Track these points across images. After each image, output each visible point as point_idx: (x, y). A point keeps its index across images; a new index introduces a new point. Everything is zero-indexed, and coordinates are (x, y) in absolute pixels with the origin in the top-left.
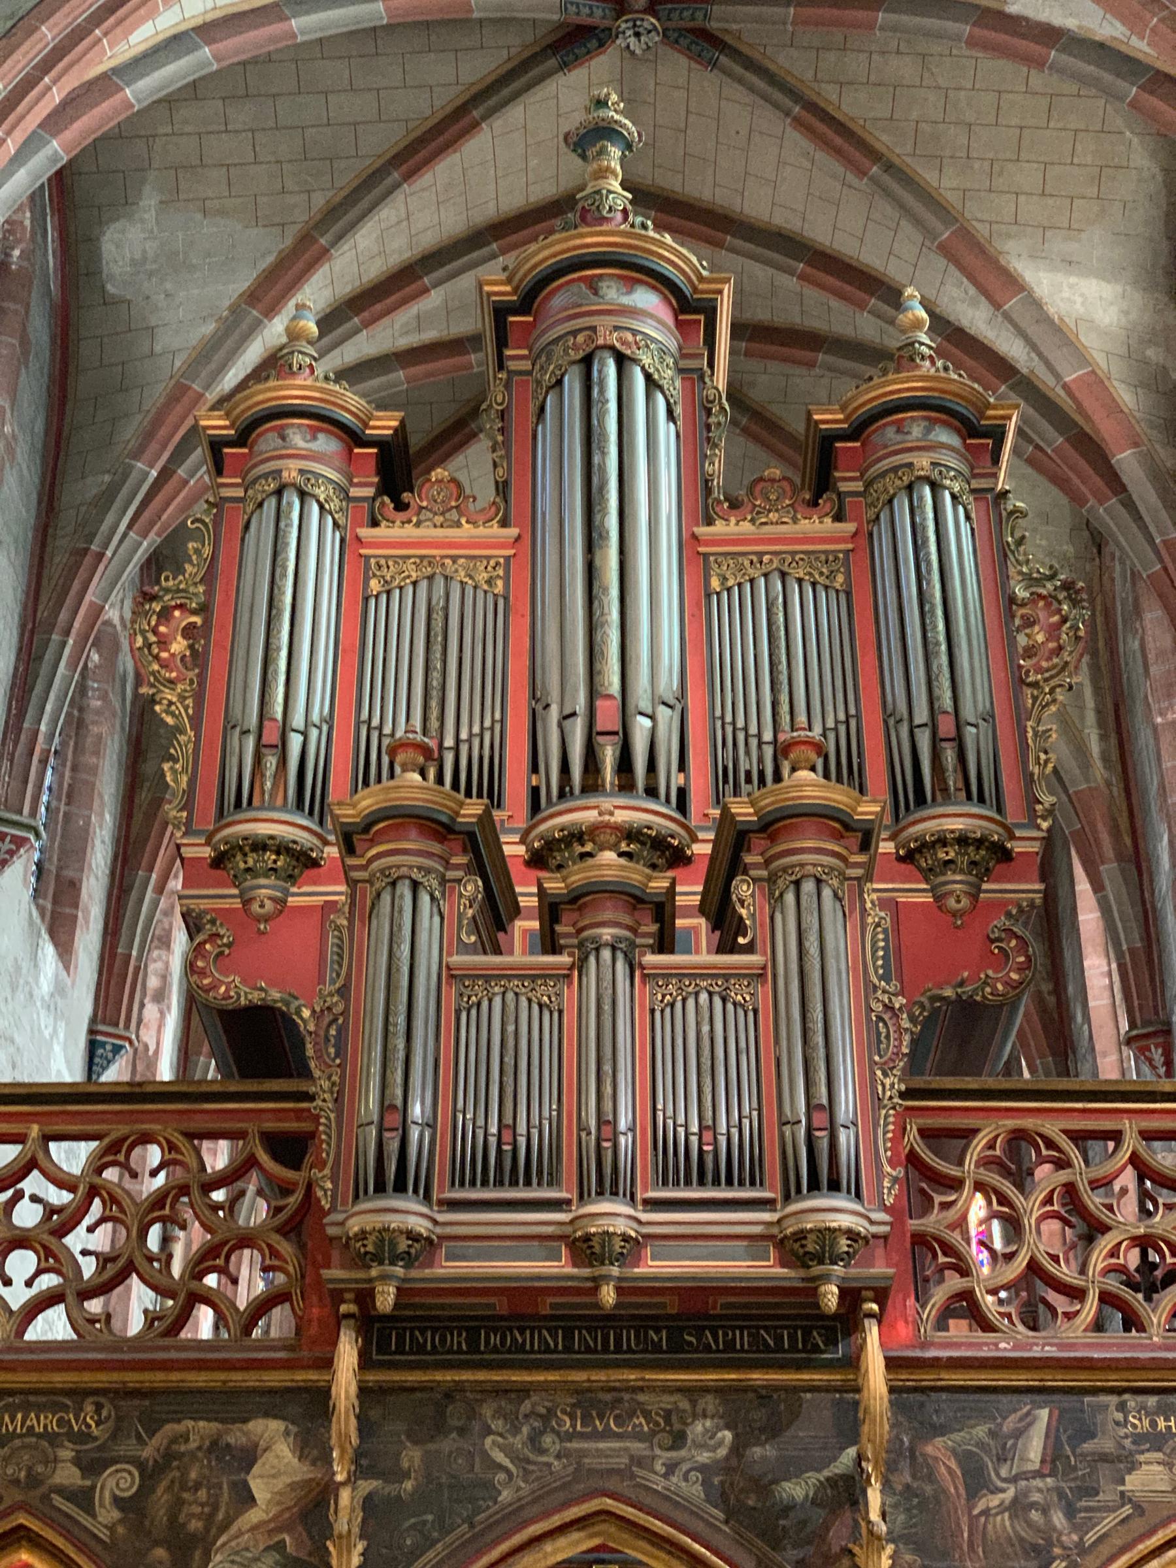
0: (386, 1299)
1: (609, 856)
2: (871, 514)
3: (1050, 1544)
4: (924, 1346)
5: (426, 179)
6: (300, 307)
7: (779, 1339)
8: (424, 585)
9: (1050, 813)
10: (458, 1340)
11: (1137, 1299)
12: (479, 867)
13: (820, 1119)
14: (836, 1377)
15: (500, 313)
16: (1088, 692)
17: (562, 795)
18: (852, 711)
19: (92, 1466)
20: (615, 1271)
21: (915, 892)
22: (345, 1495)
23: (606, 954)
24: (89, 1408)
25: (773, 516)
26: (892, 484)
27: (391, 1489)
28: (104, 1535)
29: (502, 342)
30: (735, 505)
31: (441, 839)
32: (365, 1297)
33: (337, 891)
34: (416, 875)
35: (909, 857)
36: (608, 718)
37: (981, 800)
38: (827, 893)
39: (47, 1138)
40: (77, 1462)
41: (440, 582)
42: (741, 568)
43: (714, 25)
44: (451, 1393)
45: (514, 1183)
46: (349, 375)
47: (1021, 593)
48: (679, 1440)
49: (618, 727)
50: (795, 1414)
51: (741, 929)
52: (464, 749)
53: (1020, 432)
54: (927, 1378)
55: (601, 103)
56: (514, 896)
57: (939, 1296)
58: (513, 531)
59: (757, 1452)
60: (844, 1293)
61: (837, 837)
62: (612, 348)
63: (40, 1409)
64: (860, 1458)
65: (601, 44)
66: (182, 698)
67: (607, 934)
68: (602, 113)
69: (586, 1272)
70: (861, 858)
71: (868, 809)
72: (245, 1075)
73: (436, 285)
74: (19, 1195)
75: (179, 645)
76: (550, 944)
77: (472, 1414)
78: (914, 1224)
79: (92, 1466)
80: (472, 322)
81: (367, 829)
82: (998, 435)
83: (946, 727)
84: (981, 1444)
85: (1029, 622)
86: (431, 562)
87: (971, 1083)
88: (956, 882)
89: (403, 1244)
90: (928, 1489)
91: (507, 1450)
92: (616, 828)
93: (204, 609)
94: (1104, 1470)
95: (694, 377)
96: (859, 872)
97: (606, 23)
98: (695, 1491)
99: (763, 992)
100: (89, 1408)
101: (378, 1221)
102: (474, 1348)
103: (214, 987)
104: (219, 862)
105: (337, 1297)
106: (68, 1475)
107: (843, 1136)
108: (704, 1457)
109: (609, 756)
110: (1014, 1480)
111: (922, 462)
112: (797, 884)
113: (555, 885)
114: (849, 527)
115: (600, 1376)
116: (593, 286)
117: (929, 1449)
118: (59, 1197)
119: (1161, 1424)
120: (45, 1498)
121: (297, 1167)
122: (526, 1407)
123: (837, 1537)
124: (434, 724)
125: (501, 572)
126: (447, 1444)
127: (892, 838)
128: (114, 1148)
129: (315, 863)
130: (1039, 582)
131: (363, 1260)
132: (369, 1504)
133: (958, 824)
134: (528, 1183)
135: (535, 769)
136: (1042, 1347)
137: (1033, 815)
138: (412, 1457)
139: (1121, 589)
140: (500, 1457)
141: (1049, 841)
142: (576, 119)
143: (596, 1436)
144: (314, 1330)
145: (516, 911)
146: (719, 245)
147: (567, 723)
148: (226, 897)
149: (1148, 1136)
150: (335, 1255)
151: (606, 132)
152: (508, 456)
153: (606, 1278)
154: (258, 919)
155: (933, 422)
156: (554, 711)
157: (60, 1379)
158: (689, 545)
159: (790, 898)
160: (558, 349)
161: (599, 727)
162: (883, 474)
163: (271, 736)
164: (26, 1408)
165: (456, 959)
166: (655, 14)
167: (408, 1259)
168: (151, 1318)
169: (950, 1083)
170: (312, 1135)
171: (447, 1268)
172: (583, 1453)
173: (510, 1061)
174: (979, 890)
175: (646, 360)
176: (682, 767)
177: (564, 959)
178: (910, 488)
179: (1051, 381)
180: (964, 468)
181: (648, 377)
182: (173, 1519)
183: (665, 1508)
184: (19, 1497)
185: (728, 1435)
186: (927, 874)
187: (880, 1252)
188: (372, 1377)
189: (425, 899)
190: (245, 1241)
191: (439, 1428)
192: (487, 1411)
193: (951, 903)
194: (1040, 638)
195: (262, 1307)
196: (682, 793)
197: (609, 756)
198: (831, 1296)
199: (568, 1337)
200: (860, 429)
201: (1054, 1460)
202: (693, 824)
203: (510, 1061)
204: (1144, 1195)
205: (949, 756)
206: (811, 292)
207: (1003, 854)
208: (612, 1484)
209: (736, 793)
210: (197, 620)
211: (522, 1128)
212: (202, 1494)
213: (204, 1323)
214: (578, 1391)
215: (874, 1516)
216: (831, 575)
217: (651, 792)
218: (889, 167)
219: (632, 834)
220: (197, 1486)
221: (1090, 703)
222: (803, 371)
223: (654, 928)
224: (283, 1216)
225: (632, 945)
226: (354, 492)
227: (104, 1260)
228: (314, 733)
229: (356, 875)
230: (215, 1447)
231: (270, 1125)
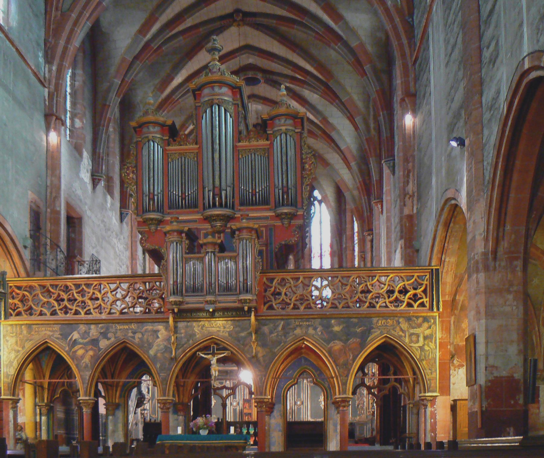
0: (176, 310)
18: (268, 184)
32: (173, 310)
42: (245, 152)
57: (267, 305)
74: (117, 293)
78: (264, 294)
88: (286, 222)
89: (178, 303)
104: (144, 222)
105: (169, 310)
114: (268, 142)
118: (124, 293)
119: (301, 323)
125: (196, 156)
136: (284, 312)
147: (209, 192)
148: (146, 229)
156: (207, 189)
158: (234, 147)
174: (290, 222)
181: (225, 110)
198: (246, 308)
216: (265, 153)
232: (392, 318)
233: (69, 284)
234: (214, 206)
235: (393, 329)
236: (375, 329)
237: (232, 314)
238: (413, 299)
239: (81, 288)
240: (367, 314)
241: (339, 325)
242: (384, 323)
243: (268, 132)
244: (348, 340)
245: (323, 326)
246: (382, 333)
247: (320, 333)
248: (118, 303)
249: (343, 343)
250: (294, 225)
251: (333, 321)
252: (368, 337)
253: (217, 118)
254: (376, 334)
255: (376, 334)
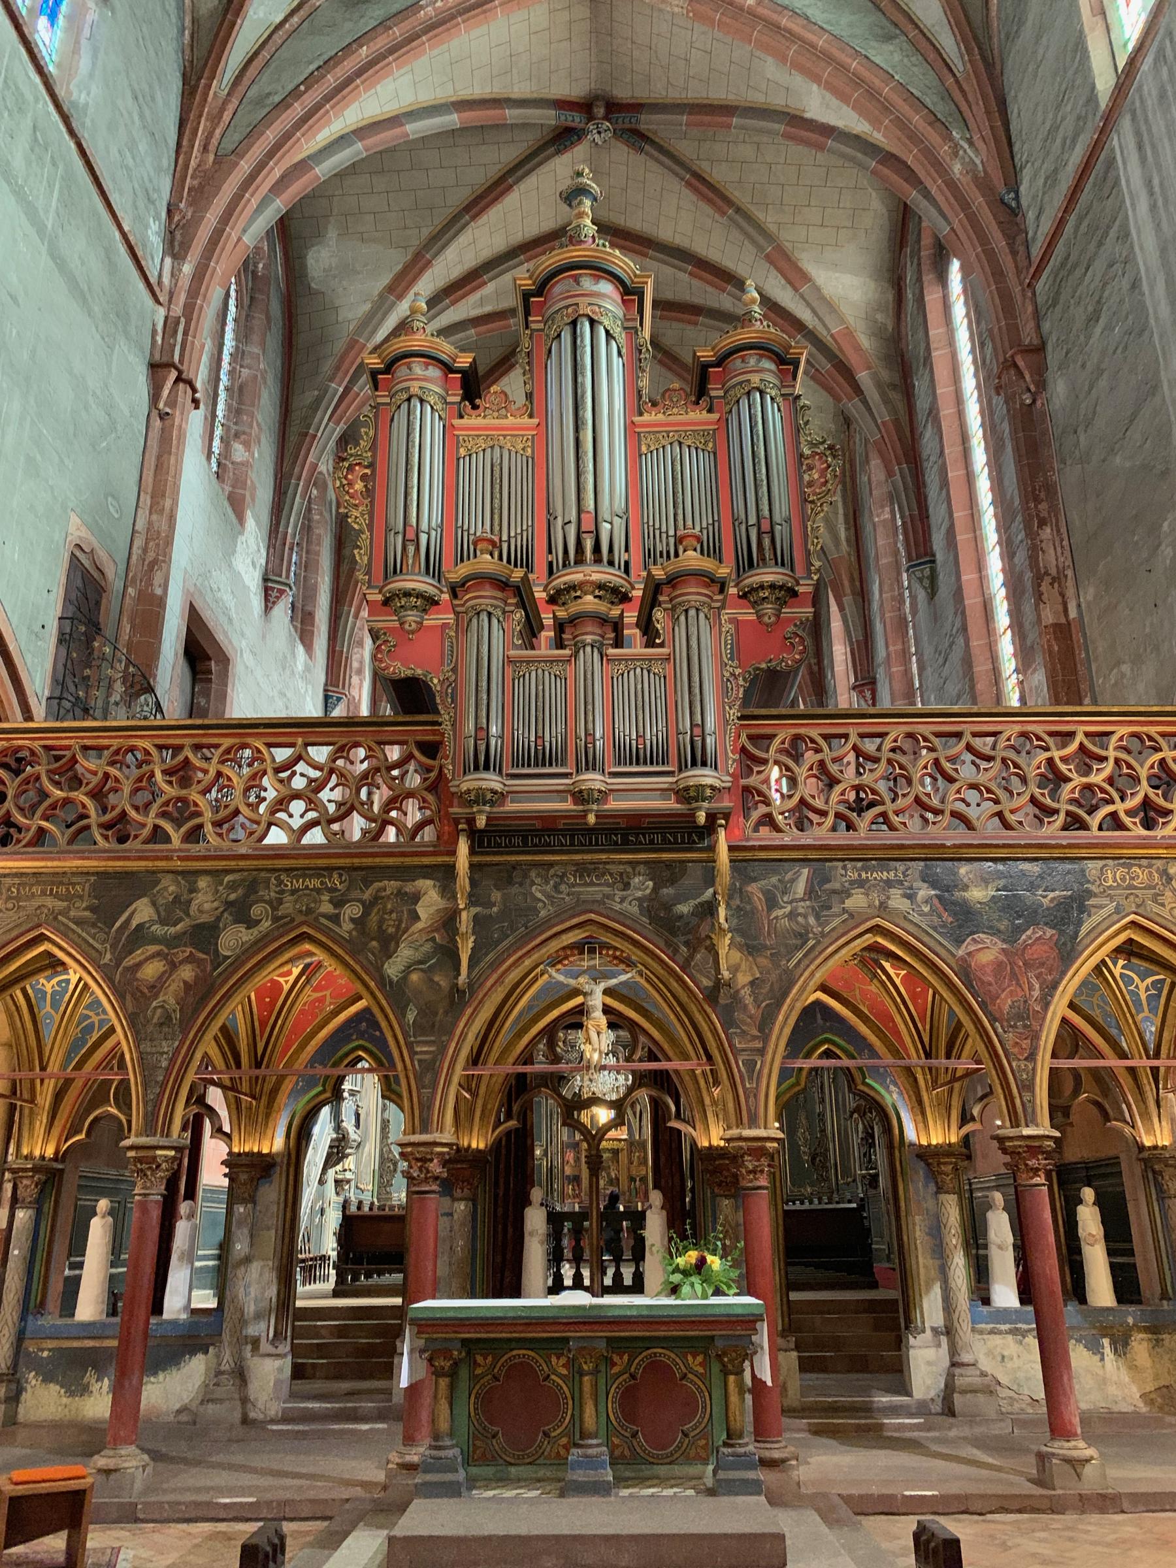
0: (481, 822)
1: (589, 598)
2: (728, 408)
3: (807, 932)
4: (748, 840)
5: (484, 219)
6: (416, 294)
7: (676, 838)
8: (489, 451)
9: (818, 570)
10: (517, 841)
11: (853, 816)
12: (522, 604)
13: (697, 731)
14: (704, 855)
15: (526, 296)
16: (840, 505)
17: (564, 566)
19: (338, 903)
20: (595, 807)
21: (747, 614)
22: (464, 915)
23: (588, 649)
24: (335, 876)
25: (675, 410)
26: (739, 392)
27: (487, 911)
28: (346, 936)
29: (527, 313)
30: (654, 404)
31: (502, 590)
32: (471, 821)
33: (449, 618)
34: (490, 609)
35: (744, 596)
36: (588, 524)
37: (783, 565)
38: (702, 615)
39: (307, 745)
40: (331, 901)
41: (497, 450)
42: (658, 440)
43: (642, 127)
44: (515, 866)
45: (544, 765)
46: (444, 332)
47: (807, 452)
48: (627, 886)
49: (593, 528)
50: (684, 872)
51: (658, 635)
52: (513, 541)
53: (808, 361)
54: (748, 855)
55: (579, 174)
56: (541, 620)
57: (755, 815)
58: (535, 421)
59: (665, 891)
60: (708, 816)
61: (707, 586)
62: (588, 316)
63: (310, 877)
64: (715, 893)
65: (579, 139)
66: (362, 515)
67: (589, 639)
68: (580, 180)
69: (581, 808)
70: (720, 597)
71: (724, 571)
72: (407, 711)
73: (491, 280)
74: (294, 773)
75: (359, 486)
76: (560, 644)
77: (525, 876)
79: (338, 903)
80: (511, 301)
81: (463, 585)
82: (796, 363)
83: (765, 526)
84: (775, 886)
85: (810, 468)
86: (492, 438)
87: (774, 711)
88: (769, 609)
89: (489, 796)
90: (748, 907)
91: (543, 892)
92: (592, 583)
93: (371, 465)
94: (835, 898)
95: (632, 331)
96: (718, 605)
97: (582, 125)
98: (634, 909)
99: (669, 667)
100: (335, 876)
101: (476, 784)
102: (525, 844)
103: (387, 668)
104: (386, 602)
105: (457, 822)
106: (326, 908)
107: (708, 740)
108: (639, 894)
109: (589, 544)
110: (791, 902)
111: (755, 379)
112: (686, 611)
113: (562, 614)
114: (715, 416)
115: (588, 857)
116: (576, 279)
117: (749, 889)
119: (864, 875)
120: (316, 919)
121: (434, 758)
122: (552, 872)
123: (704, 930)
124: (497, 528)
126: (515, 889)
127: (736, 585)
128: (341, 749)
129: (437, 603)
130: (816, 445)
131: (470, 803)
132: (476, 918)
133: (769, 578)
134: (551, 765)
135: (550, 552)
136: (806, 839)
137: (809, 572)
138: (496, 896)
139: (859, 449)
140: (539, 895)
141: (817, 587)
142: (565, 184)
143: (586, 885)
144: (446, 837)
145: (542, 627)
146: (645, 255)
148: (391, 621)
149: (862, 736)
150: (456, 801)
151: (581, 191)
152: (532, 378)
153: (591, 811)
154: (409, 632)
155: (761, 356)
157: (321, 862)
159: (682, 618)
160: (558, 317)
161: (583, 529)
162: (734, 386)
163: (411, 535)
164: (304, 876)
165: (512, 653)
166: (609, 120)
167: (492, 803)
168: (365, 832)
169: (763, 712)
170: (441, 743)
171: (510, 807)
172: (580, 893)
173: (540, 704)
175: (606, 323)
176: (627, 550)
177: (567, 652)
178: (748, 393)
179: (825, 333)
180: (777, 382)
181: (607, 332)
182: (380, 927)
183: (621, 918)
184: (303, 918)
185: (651, 884)
186: (754, 604)
187: (726, 796)
188: (477, 859)
189: (495, 621)
190: (410, 794)
191: (510, 882)
192: (533, 874)
193: (766, 619)
194: (816, 476)
195: (420, 826)
196: (627, 563)
197: (589, 544)
199: (572, 837)
200: (721, 361)
201: (810, 893)
202: (632, 580)
203: (540, 704)
204: (858, 765)
205: (767, 542)
206: (696, 283)
207: (793, 593)
208: (595, 907)
209: (655, 563)
210: (368, 471)
211: (547, 738)
212: (394, 916)
213: (391, 835)
214: (577, 864)
215: (722, 920)
217: (611, 563)
218: (738, 210)
219: (601, 586)
220: (391, 912)
221: (841, 511)
222: (689, 327)
223: (613, 635)
224: (428, 783)
225: (602, 644)
226: (449, 399)
227: (339, 805)
228: (433, 533)
229: (458, 609)
230: (400, 893)
231: (419, 738)
232: (1144, 862)
233: (140, 743)
234: (580, 560)
235: (1155, 901)
236: (1096, 895)
237: (652, 842)
238: (1152, 814)
239: (180, 758)
240: (1070, 846)
241: (985, 881)
242: (1123, 879)
243: (713, 393)
244: (1020, 930)
245: (934, 885)
246: (1117, 910)
247: (926, 909)
248: (297, 806)
249: (1004, 941)
250: (790, 620)
251: (964, 870)
252: (1080, 923)
253: (588, 349)
254: (1104, 912)
255: (1104, 912)
